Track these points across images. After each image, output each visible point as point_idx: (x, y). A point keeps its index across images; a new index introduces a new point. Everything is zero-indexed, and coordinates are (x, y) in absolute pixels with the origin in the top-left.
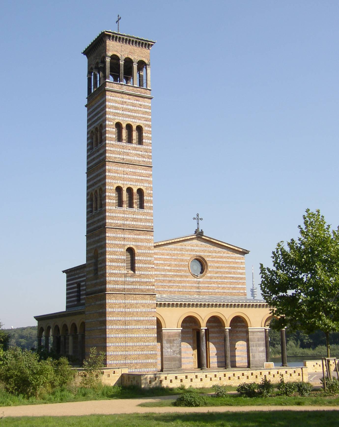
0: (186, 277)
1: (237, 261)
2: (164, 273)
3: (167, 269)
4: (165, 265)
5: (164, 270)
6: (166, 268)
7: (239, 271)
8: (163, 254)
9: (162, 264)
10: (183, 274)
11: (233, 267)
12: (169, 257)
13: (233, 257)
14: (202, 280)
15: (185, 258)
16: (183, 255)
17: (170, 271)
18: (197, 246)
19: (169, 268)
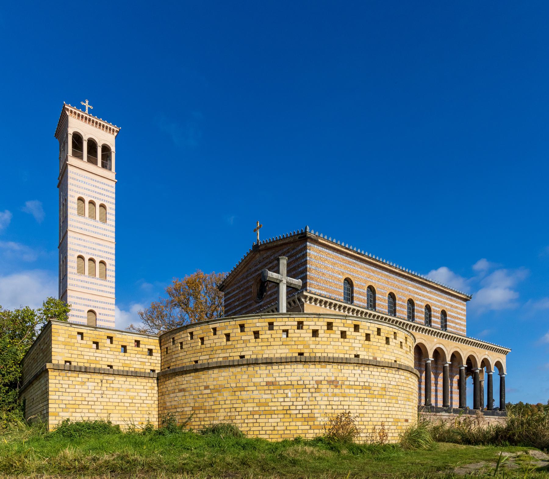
0: (250, 305)
1: (298, 256)
2: (234, 311)
3: (236, 305)
4: (234, 302)
5: (235, 307)
6: (236, 304)
7: (299, 270)
8: (234, 291)
9: (233, 301)
10: (248, 303)
11: (294, 267)
12: (238, 291)
13: (293, 254)
14: (263, 302)
15: (250, 284)
16: (248, 281)
17: (238, 306)
18: (260, 263)
19: (237, 303)
